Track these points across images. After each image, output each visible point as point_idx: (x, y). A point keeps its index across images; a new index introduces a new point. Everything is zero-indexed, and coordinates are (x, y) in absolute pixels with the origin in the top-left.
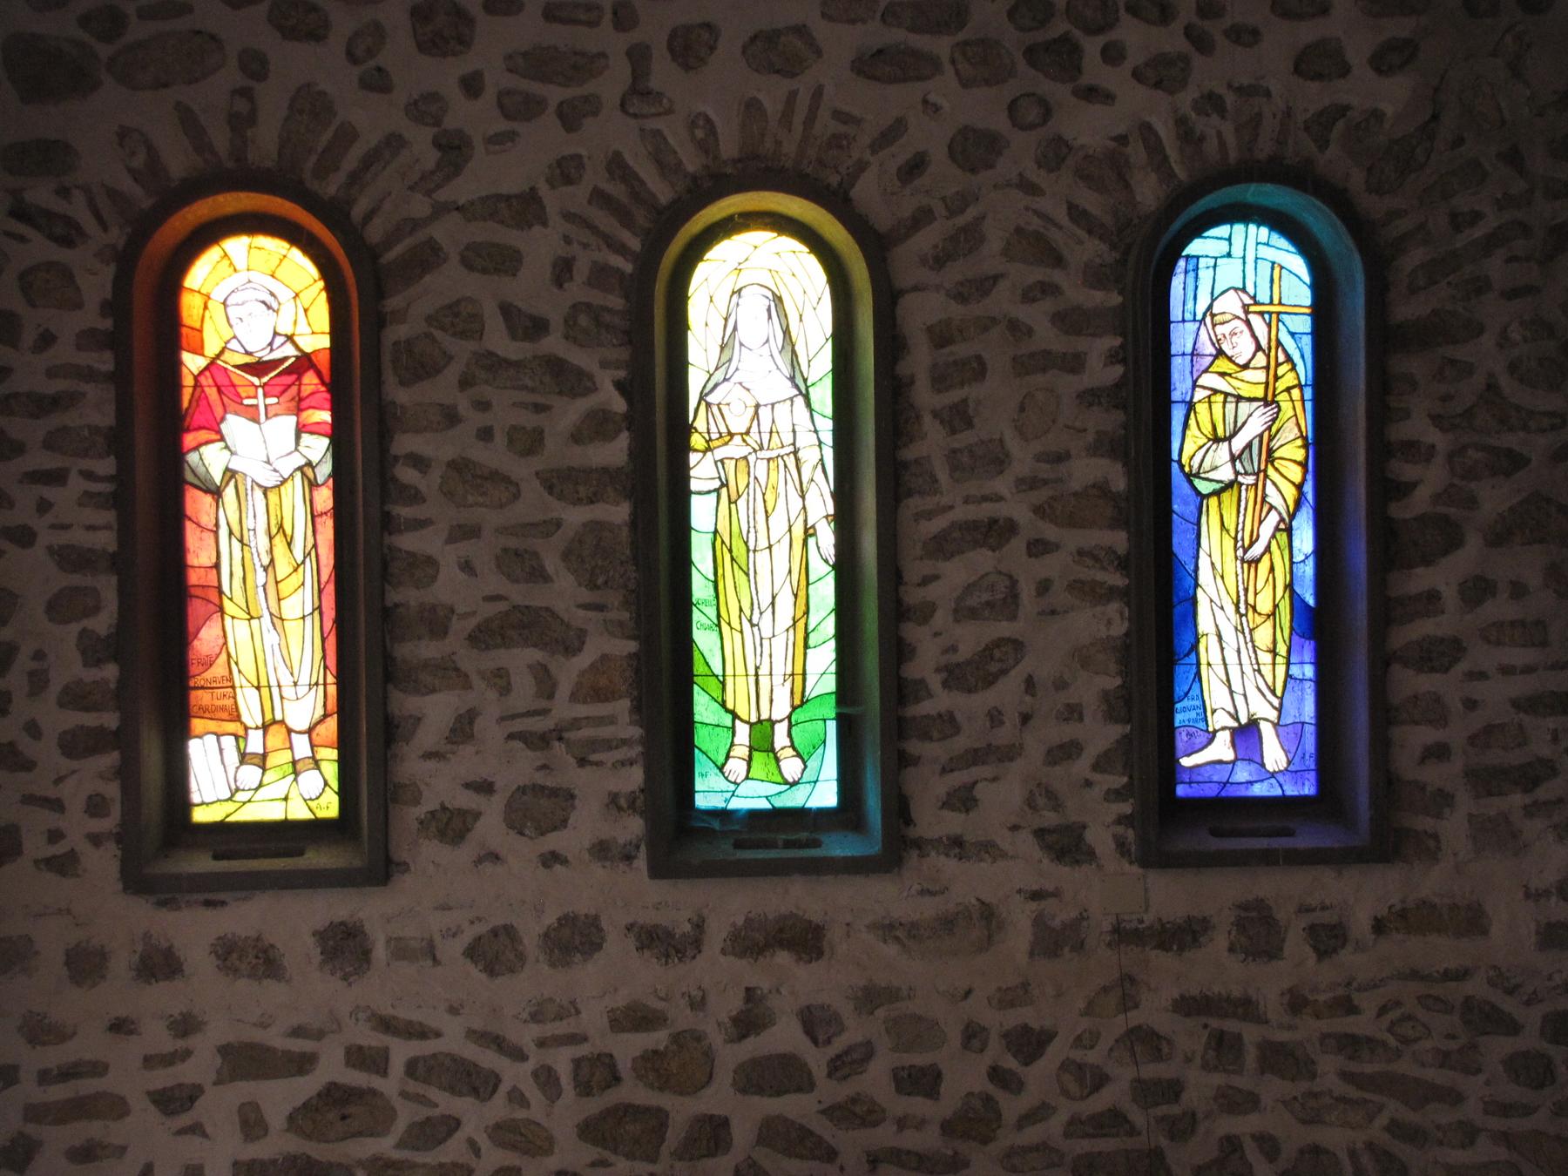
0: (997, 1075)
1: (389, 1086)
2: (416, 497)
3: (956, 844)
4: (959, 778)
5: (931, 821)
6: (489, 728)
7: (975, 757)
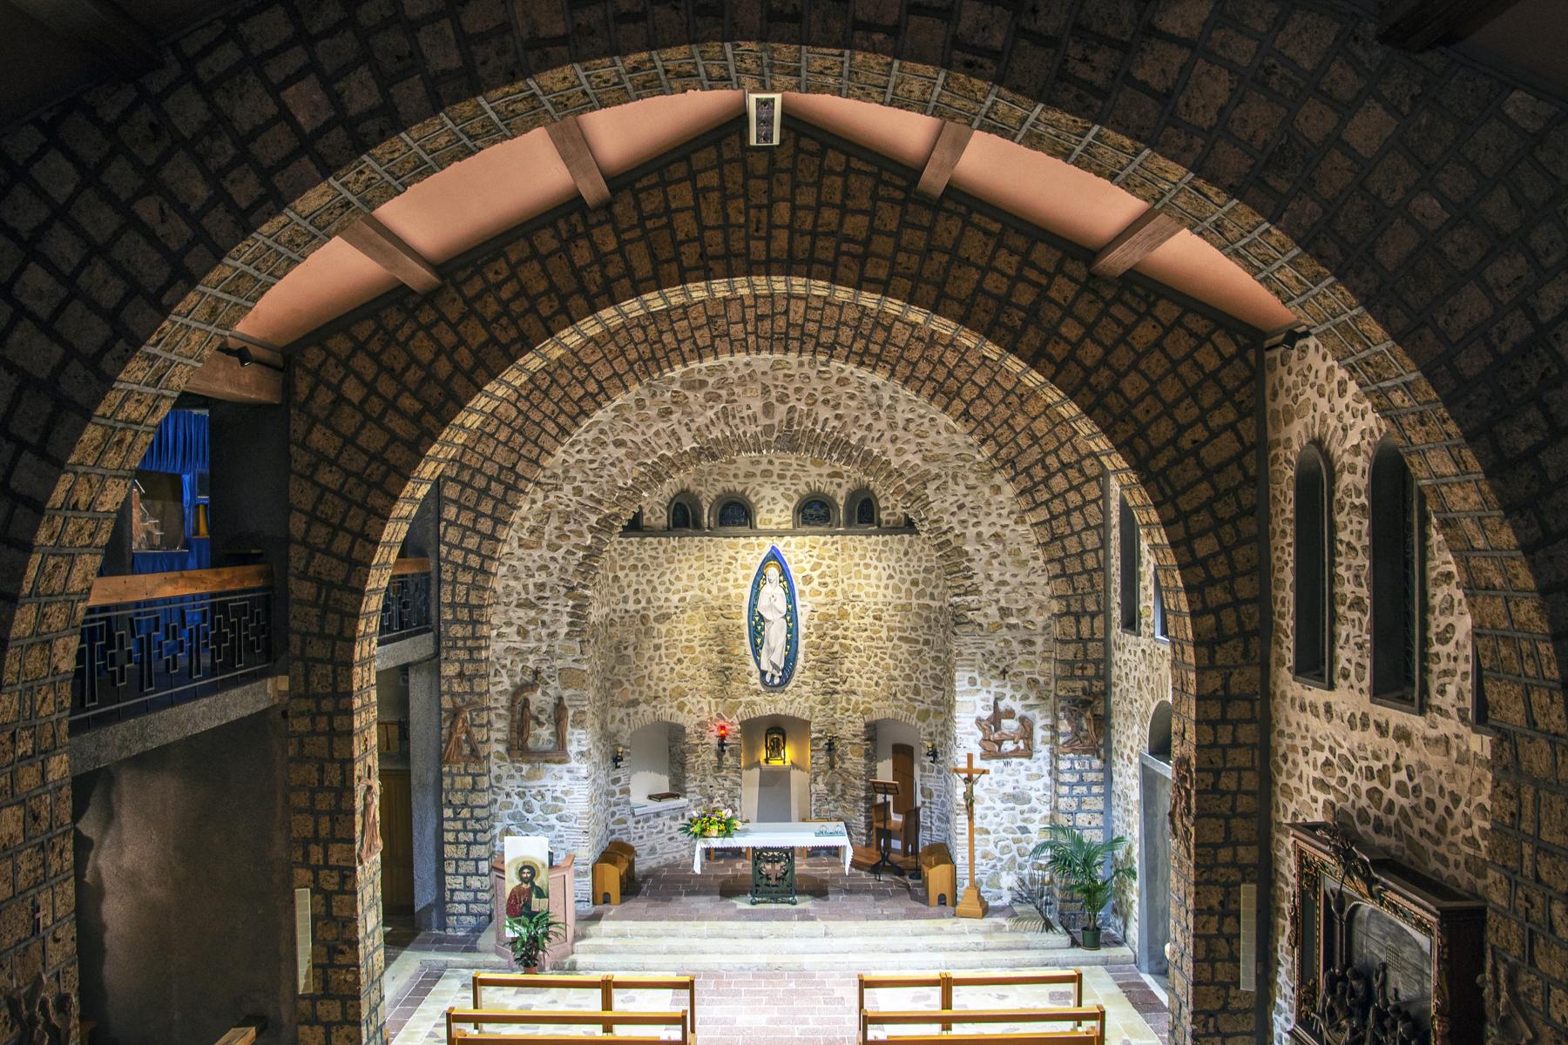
0: (1447, 809)
1: (1335, 761)
2: (1340, 554)
3: (1439, 710)
4: (1443, 680)
5: (1436, 700)
6: (1352, 641)
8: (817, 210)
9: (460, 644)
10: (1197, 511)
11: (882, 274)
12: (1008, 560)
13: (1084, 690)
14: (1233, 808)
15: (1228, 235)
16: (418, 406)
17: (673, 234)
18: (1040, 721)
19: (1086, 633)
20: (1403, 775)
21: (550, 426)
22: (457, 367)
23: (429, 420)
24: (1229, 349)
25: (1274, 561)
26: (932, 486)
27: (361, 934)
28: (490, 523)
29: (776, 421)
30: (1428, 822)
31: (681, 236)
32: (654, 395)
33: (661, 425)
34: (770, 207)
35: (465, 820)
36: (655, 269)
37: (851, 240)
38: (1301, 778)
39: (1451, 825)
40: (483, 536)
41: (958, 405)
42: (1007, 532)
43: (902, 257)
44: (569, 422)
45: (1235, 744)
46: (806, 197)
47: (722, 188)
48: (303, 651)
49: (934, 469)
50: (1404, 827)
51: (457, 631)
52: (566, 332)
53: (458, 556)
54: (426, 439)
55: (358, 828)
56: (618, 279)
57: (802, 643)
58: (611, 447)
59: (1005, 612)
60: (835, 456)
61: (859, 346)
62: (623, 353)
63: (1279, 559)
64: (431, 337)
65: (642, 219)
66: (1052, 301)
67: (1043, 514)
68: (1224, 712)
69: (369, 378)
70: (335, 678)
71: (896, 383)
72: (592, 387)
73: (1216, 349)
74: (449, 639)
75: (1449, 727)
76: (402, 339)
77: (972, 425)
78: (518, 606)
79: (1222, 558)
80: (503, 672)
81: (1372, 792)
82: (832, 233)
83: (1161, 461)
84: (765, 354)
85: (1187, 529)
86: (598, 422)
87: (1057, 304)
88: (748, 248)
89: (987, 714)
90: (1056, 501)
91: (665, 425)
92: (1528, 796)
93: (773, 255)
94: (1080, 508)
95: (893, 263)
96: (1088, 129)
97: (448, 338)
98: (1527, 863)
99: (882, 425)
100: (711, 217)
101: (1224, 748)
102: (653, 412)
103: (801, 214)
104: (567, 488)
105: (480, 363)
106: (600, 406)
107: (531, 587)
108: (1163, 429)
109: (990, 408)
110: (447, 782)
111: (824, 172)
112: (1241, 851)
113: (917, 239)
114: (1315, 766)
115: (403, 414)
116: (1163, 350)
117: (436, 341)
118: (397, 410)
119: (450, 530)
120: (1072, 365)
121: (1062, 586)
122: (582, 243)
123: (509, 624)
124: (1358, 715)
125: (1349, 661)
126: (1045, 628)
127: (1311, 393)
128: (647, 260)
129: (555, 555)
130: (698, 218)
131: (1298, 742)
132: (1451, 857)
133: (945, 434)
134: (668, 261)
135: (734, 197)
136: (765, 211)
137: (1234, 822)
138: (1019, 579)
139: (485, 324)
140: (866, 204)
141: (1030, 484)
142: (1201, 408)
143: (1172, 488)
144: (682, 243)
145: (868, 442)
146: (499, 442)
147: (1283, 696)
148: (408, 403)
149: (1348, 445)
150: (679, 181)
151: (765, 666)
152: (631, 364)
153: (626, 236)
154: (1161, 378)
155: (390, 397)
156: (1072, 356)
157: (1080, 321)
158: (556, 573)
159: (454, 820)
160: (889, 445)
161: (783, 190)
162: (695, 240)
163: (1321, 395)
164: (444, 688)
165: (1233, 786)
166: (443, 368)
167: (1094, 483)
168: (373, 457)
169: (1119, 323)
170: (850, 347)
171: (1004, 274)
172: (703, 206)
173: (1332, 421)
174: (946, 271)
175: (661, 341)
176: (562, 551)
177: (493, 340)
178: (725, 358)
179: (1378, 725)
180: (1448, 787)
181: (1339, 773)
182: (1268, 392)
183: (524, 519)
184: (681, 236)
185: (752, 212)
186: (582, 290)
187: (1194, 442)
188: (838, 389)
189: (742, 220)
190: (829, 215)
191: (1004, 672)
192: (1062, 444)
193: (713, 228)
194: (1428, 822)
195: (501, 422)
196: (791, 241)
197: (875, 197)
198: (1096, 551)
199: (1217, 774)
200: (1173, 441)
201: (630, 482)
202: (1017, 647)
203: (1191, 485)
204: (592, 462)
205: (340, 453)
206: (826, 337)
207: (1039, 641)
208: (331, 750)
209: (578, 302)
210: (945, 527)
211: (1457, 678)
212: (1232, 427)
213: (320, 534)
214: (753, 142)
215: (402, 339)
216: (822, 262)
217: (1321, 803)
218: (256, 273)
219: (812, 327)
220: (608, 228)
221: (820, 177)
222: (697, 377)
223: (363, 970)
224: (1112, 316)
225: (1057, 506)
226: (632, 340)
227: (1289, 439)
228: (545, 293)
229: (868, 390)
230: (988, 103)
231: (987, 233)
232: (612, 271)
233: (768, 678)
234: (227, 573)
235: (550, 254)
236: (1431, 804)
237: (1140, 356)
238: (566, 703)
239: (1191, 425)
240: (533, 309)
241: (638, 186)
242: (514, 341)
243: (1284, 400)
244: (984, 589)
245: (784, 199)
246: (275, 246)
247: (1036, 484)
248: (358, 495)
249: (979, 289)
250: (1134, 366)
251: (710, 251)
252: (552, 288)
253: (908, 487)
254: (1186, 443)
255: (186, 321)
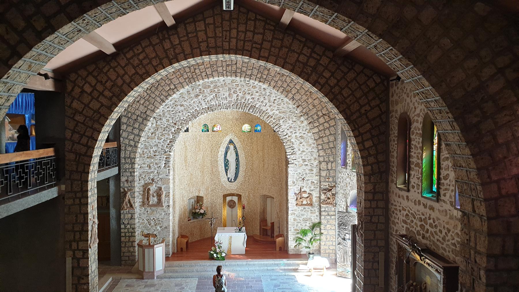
1: (410, 215)
4: (445, 192)
5: (442, 197)
6: (415, 177)
7: (446, 189)
8: (245, 32)
9: (127, 170)
10: (366, 133)
11: (266, 55)
12: (305, 144)
13: (329, 185)
14: (377, 228)
15: (378, 50)
16: (111, 94)
17: (198, 39)
18: (315, 194)
19: (330, 168)
20: (431, 221)
21: (158, 99)
22: (124, 82)
23: (115, 99)
24: (378, 80)
25: (391, 149)
26: (281, 121)
27: (90, 272)
28: (138, 131)
29: (233, 99)
30: (440, 237)
31: (200, 40)
32: (193, 89)
33: (196, 100)
34: (230, 31)
35: (128, 229)
36: (192, 51)
37: (256, 43)
38: (398, 219)
39: (447, 238)
40: (135, 135)
41: (290, 95)
42: (305, 135)
43: (273, 49)
44: (165, 98)
45: (377, 207)
46: (242, 28)
47: (214, 23)
48: (70, 176)
49: (282, 115)
50: (432, 238)
51: (127, 166)
52: (162, 71)
53: (127, 141)
54: (114, 106)
55: (90, 236)
56: (179, 54)
57: (241, 168)
58: (179, 106)
59: (304, 161)
60: (251, 111)
61: (259, 76)
62: (182, 76)
63: (392, 148)
64: (115, 71)
65: (187, 34)
66: (321, 64)
67: (316, 130)
68: (374, 197)
69: (93, 85)
70: (82, 186)
71: (271, 88)
72: (172, 87)
73: (374, 80)
74: (124, 169)
75: (447, 207)
76: (105, 71)
77: (295, 101)
78: (148, 158)
79: (374, 148)
80: (142, 179)
81: (421, 226)
82: (250, 41)
83: (355, 117)
84: (229, 78)
85: (362, 138)
86: (175, 98)
87: (322, 65)
88: (223, 44)
89: (297, 192)
90: (321, 126)
91: (196, 100)
92: (473, 234)
93: (231, 47)
94: (328, 128)
95: (270, 51)
96: (334, 14)
97: (121, 72)
98: (472, 256)
99: (267, 101)
100: (210, 34)
101: (374, 208)
102: (193, 95)
103: (240, 33)
104: (164, 120)
105: (132, 80)
106: (174, 93)
107: (152, 152)
108: (356, 107)
109: (300, 96)
110: (122, 216)
111: (248, 19)
112: (379, 241)
113: (278, 43)
114: (403, 216)
115: (106, 97)
116: (356, 81)
117: (117, 72)
118: (103, 95)
119: (124, 133)
120: (327, 85)
121: (322, 153)
122: (167, 41)
123: (144, 164)
124: (417, 201)
125: (414, 183)
126: (317, 166)
127: (405, 96)
128: (189, 48)
129: (160, 141)
130: (206, 33)
131: (398, 208)
132: (447, 249)
133: (286, 105)
134: (196, 48)
135: (218, 27)
136: (228, 32)
137: (377, 232)
138: (308, 150)
139: (134, 68)
140: (261, 31)
141: (312, 120)
142: (368, 100)
143: (358, 125)
144: (201, 42)
145: (262, 107)
146: (140, 104)
147: (393, 192)
148: (107, 93)
149: (416, 113)
150: (199, 21)
151: (229, 176)
152: (185, 79)
153: (182, 39)
154: (356, 90)
155: (101, 91)
156: (327, 82)
157: (330, 71)
158: (161, 147)
159: (125, 229)
160: (268, 108)
161: (234, 25)
162: (205, 41)
163: (408, 97)
164: (122, 185)
165: (377, 221)
166: (119, 82)
167: (333, 120)
168: (95, 112)
169: (342, 72)
170: (257, 75)
171: (306, 55)
172: (208, 29)
173: (411, 105)
174: (287, 54)
175: (195, 72)
176: (162, 140)
177: (137, 73)
178: (216, 79)
179: (424, 205)
180: (446, 226)
181: (411, 219)
182: (390, 94)
183: (150, 129)
184: (200, 40)
185: (224, 32)
186: (167, 57)
187: (366, 110)
188: (252, 89)
189: (221, 35)
190: (249, 34)
191: (303, 179)
192: (323, 108)
193: (211, 37)
194: (440, 237)
195: (141, 97)
196: (237, 43)
197: (264, 29)
198: (333, 142)
199: (371, 217)
200: (359, 110)
201: (185, 118)
202: (308, 172)
203: (364, 124)
204: (173, 111)
205: (83, 110)
206: (249, 72)
207: (315, 170)
208: (80, 210)
209: (165, 61)
210: (285, 134)
211: (450, 191)
212: (378, 106)
213: (76, 137)
214: (224, 9)
215: (105, 71)
216: (247, 50)
217: (405, 228)
218: (46, 54)
219: (245, 69)
220: (176, 36)
221: (247, 22)
222: (207, 84)
223: (90, 284)
224: (340, 69)
225: (321, 128)
226: (185, 72)
227: (397, 110)
228: (154, 58)
229: (262, 90)
230: (301, 4)
231: (300, 41)
232: (177, 51)
233: (230, 180)
234: (41, 151)
235: (156, 44)
236: (441, 231)
237: (349, 83)
238: (163, 189)
239: (365, 105)
240: (150, 63)
241: (186, 22)
242: (144, 74)
243: (395, 97)
244: (297, 153)
245: (234, 29)
246: (53, 44)
247: (315, 120)
248: (90, 124)
249: (297, 60)
250: (347, 86)
251: (210, 45)
252: (157, 55)
253: (274, 121)
254: (363, 111)
255: (19, 70)
